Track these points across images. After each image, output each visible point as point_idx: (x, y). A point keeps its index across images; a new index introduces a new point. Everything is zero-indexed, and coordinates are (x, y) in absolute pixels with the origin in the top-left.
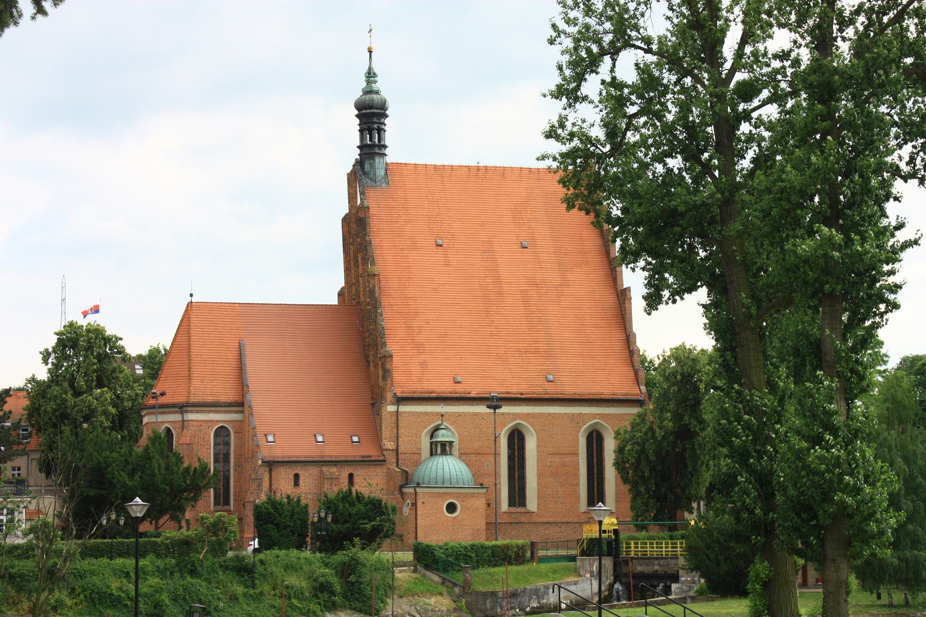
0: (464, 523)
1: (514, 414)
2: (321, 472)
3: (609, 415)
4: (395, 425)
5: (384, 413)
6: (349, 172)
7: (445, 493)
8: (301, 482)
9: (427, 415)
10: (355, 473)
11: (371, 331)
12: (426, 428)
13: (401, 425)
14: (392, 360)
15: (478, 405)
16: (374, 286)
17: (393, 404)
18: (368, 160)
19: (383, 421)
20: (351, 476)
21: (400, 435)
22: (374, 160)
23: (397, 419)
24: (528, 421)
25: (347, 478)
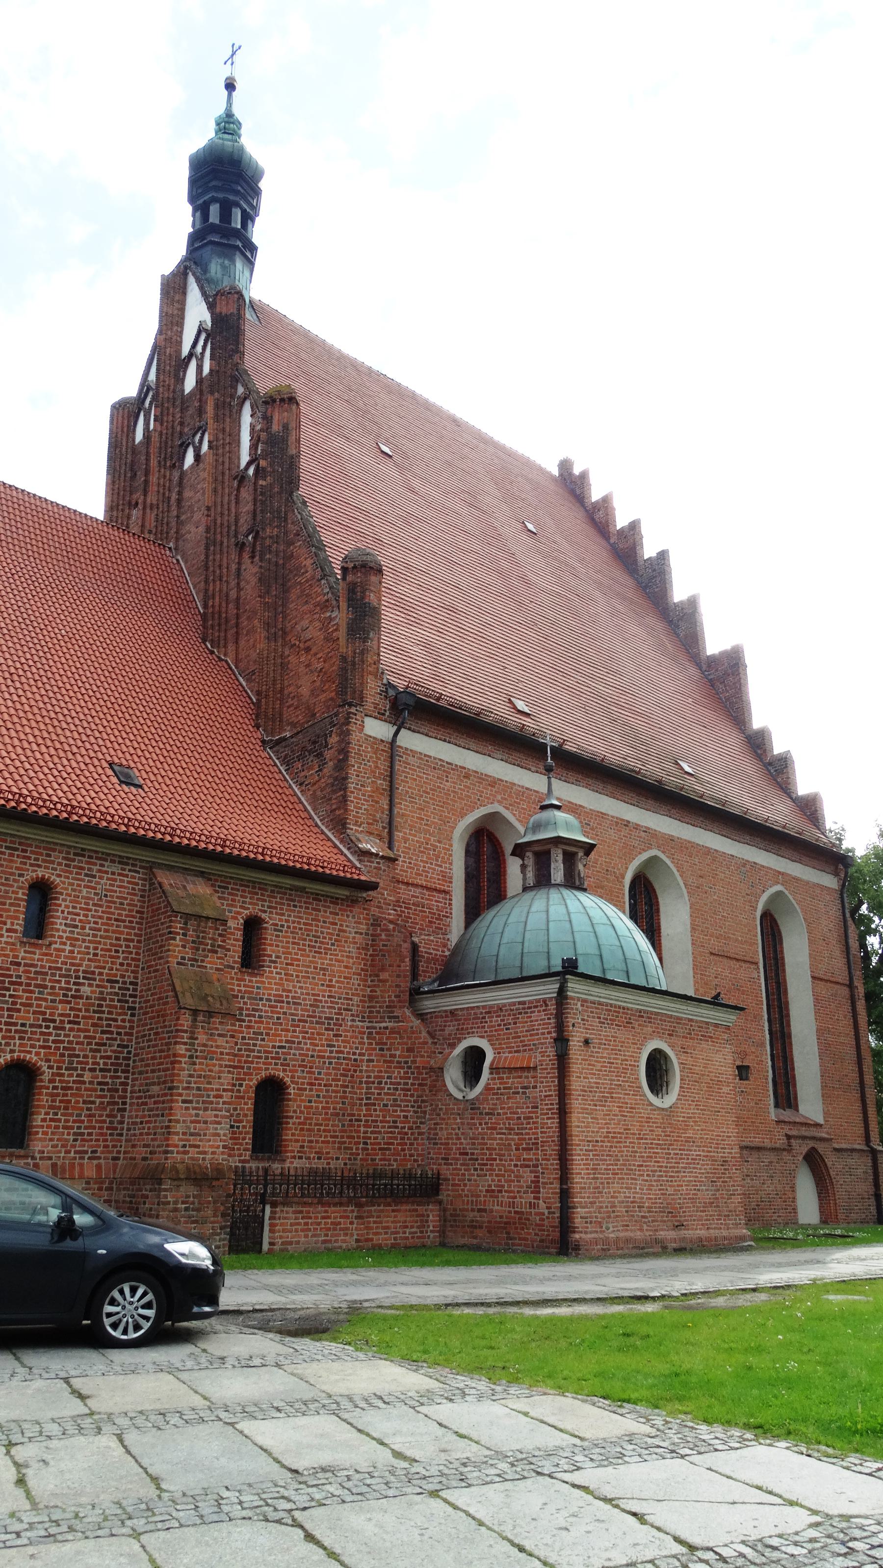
0: (690, 1133)
1: (647, 830)
2: (153, 887)
3: (797, 879)
4: (385, 785)
5: (355, 737)
6: (167, 273)
7: (640, 1014)
8: (59, 922)
9: (467, 776)
10: (270, 919)
11: (268, 542)
12: (463, 815)
13: (401, 788)
14: (380, 582)
15: (577, 783)
16: (286, 427)
17: (380, 716)
18: (220, 257)
19: (352, 761)
20: (252, 926)
21: (398, 820)
22: (233, 262)
23: (392, 767)
24: (672, 857)
25: (239, 935)
